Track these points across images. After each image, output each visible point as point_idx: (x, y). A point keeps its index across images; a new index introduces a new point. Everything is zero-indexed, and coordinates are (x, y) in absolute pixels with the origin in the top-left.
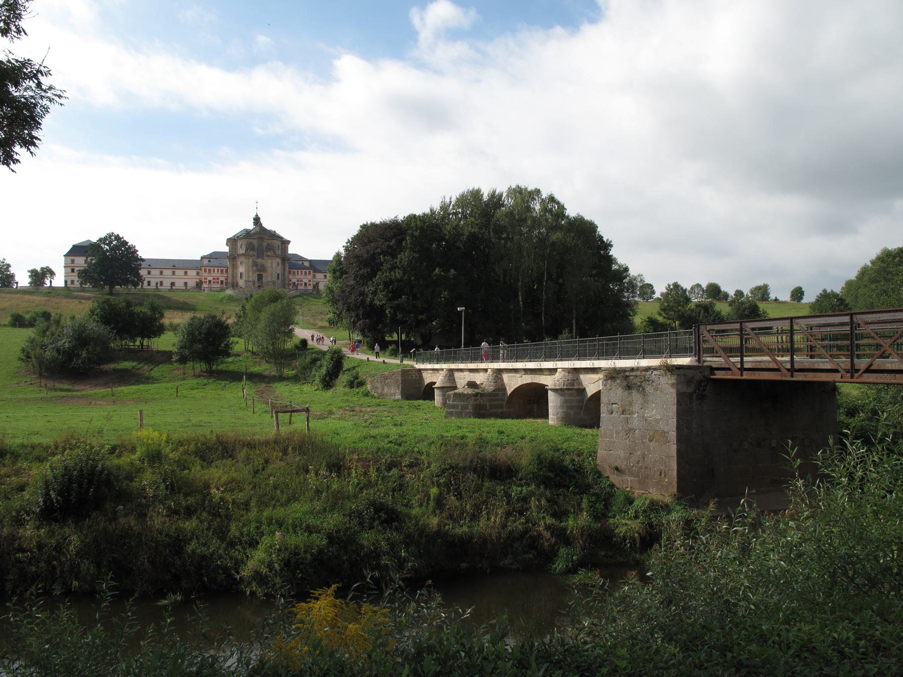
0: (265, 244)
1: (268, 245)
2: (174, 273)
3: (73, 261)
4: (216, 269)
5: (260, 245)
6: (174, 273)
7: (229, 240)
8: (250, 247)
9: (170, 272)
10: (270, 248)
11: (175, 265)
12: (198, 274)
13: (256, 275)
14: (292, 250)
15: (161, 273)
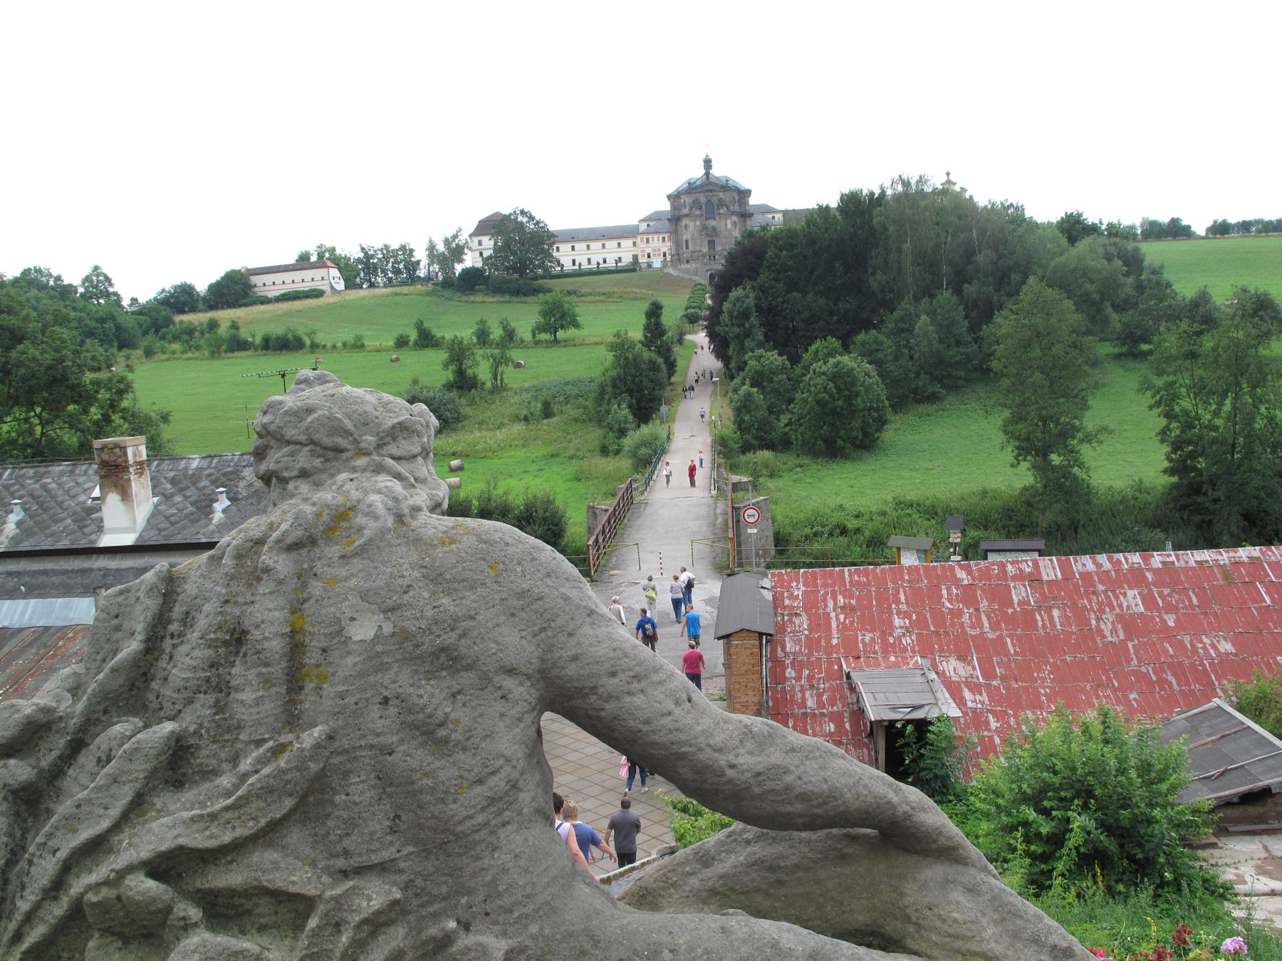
5: (709, 202)
7: (669, 197)
10: (722, 203)
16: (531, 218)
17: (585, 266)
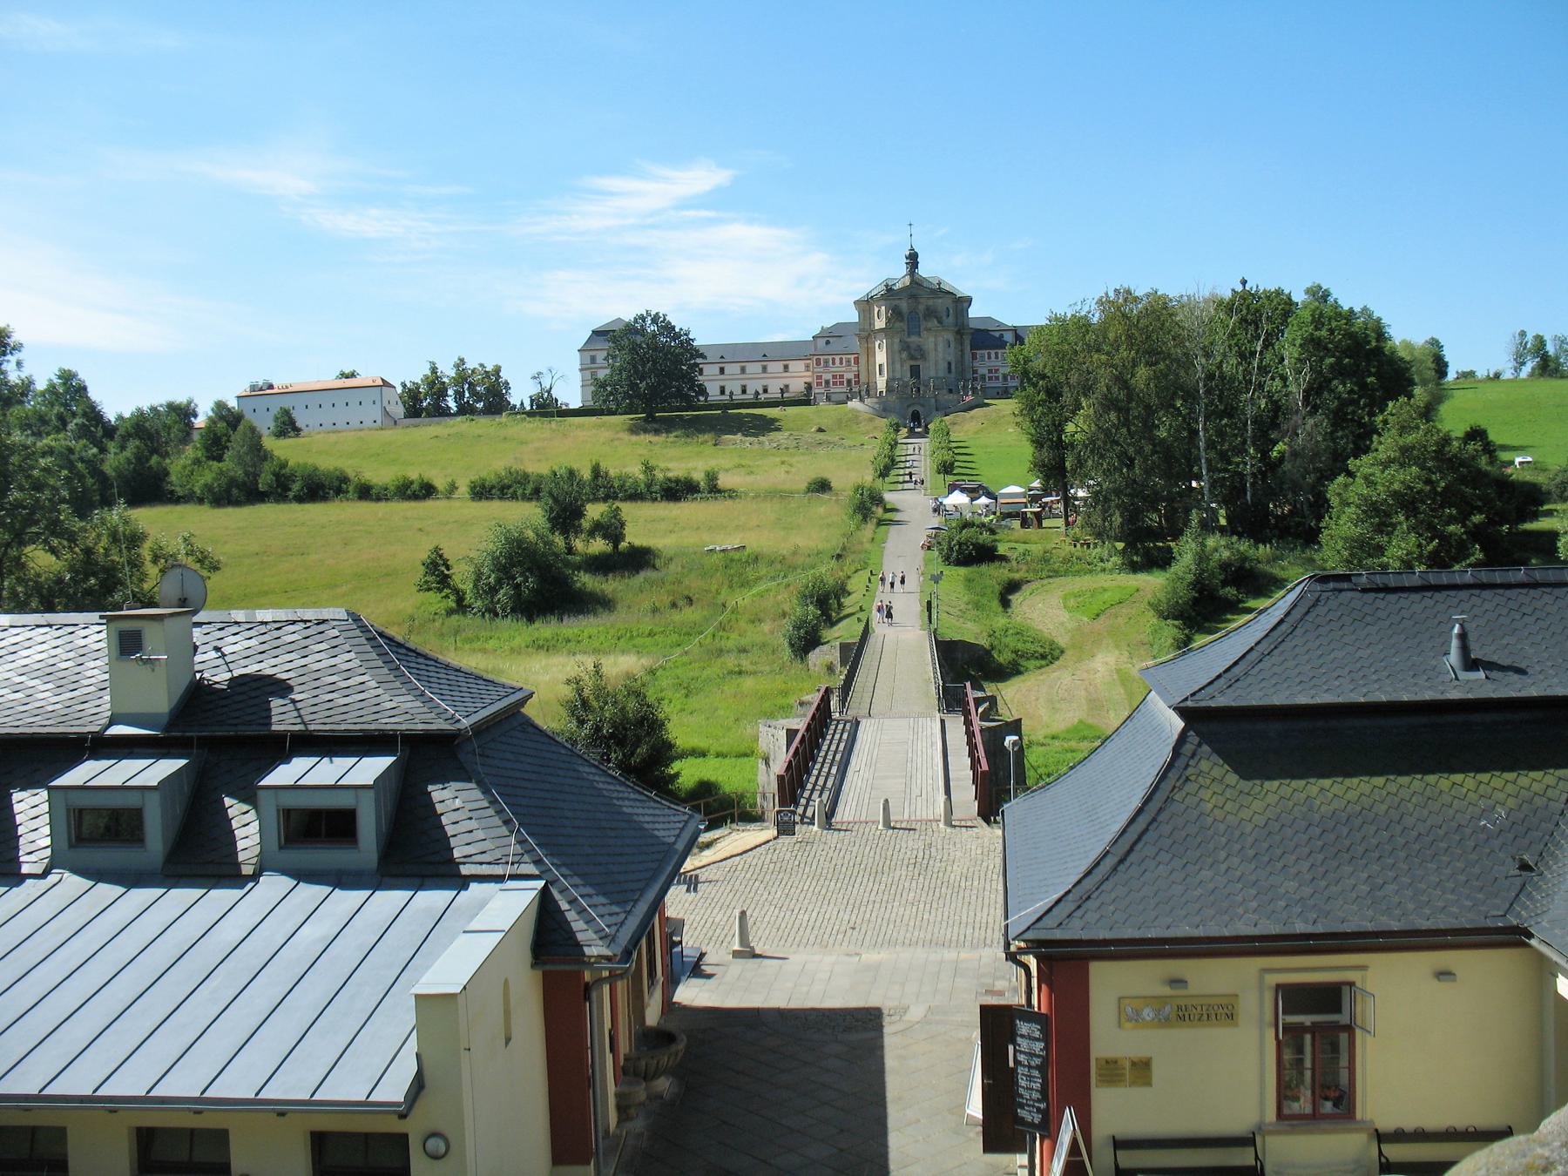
0: (921, 307)
1: (928, 309)
2: (764, 369)
3: (593, 360)
4: (837, 359)
5: (913, 312)
6: (764, 369)
8: (896, 315)
9: (757, 367)
10: (931, 313)
11: (765, 354)
12: (807, 366)
13: (907, 367)
14: (973, 312)
15: (743, 370)
16: (669, 328)
17: (738, 396)
